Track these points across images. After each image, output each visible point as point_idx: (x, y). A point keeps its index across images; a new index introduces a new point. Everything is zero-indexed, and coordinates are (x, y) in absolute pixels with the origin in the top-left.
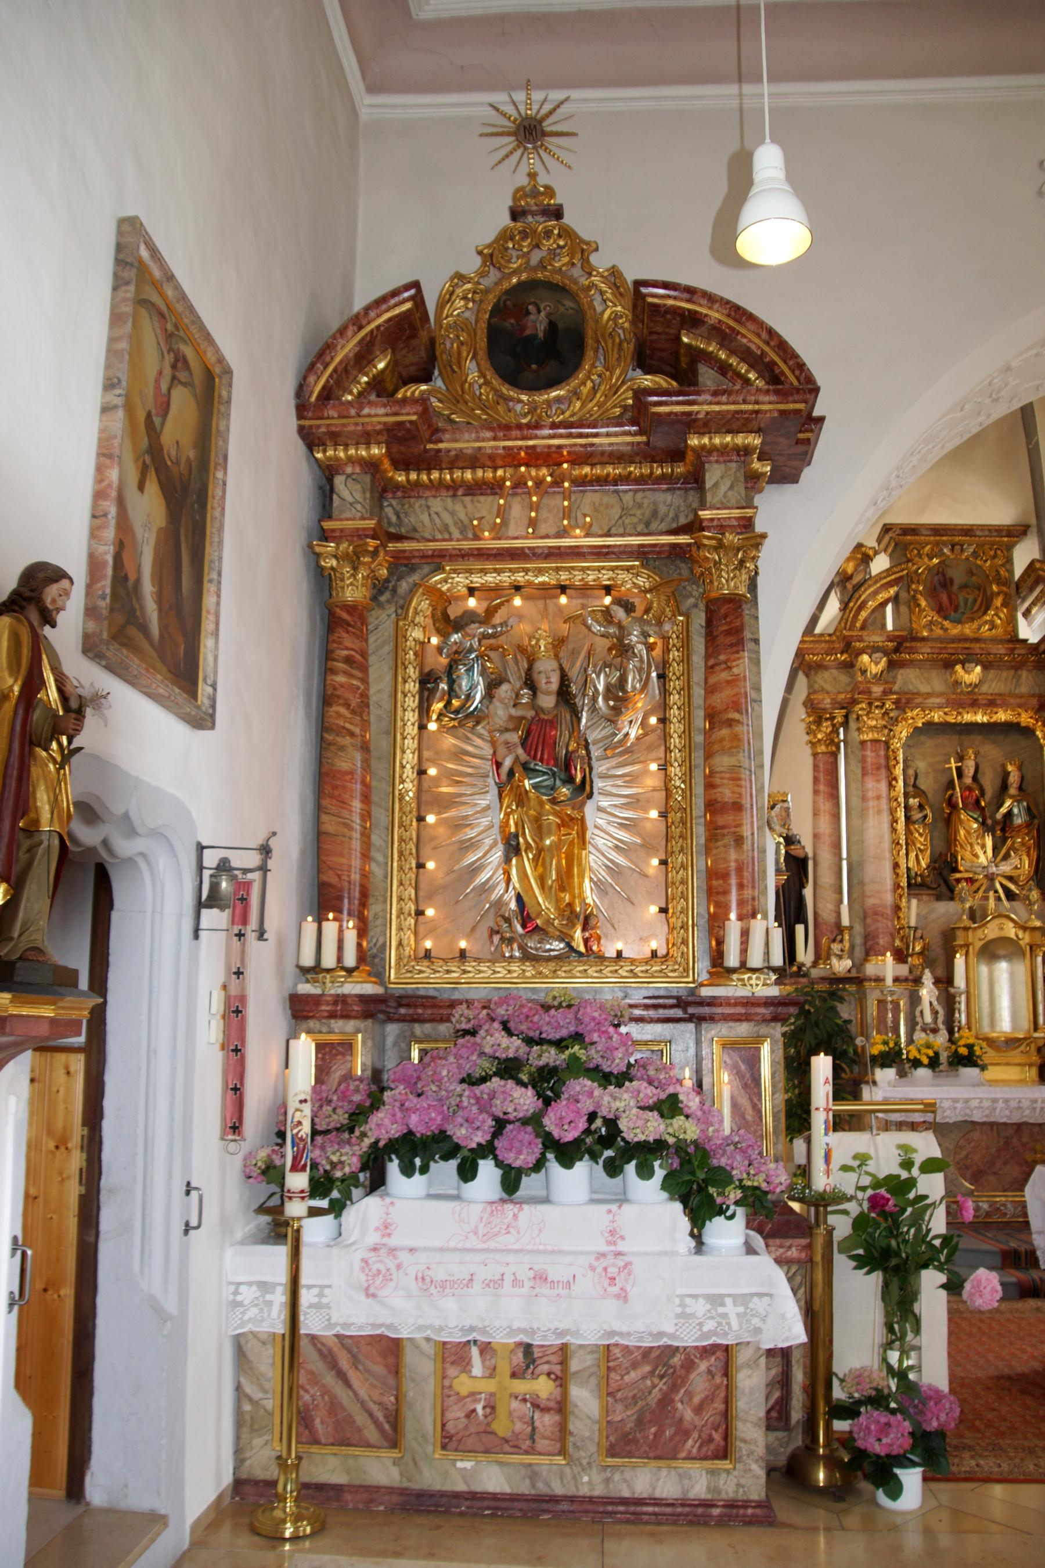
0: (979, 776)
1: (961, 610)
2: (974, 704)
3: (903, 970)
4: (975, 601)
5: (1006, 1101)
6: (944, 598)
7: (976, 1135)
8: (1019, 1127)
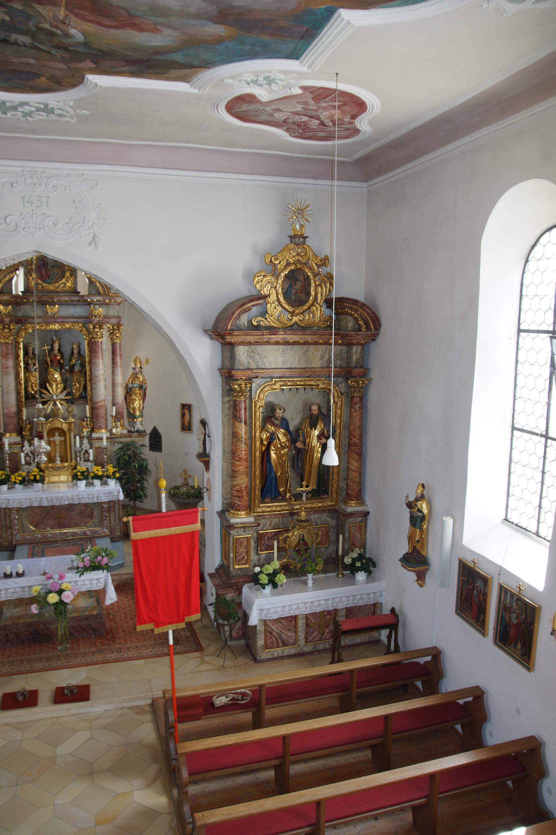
0: (62, 350)
1: (52, 278)
2: (55, 322)
3: (18, 439)
4: (58, 273)
5: (46, 498)
6: (44, 272)
7: (36, 510)
8: (53, 507)
